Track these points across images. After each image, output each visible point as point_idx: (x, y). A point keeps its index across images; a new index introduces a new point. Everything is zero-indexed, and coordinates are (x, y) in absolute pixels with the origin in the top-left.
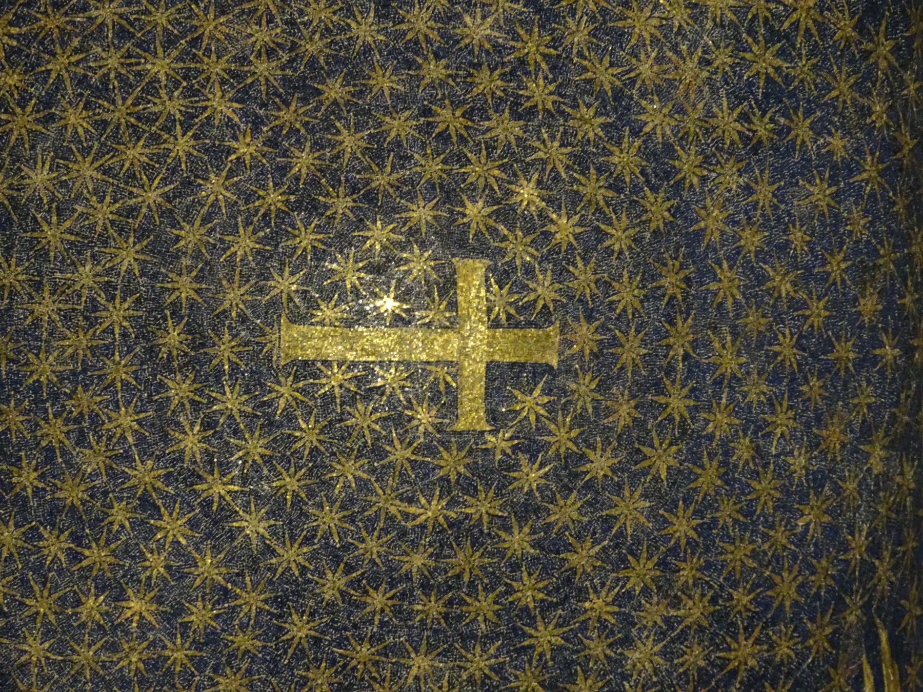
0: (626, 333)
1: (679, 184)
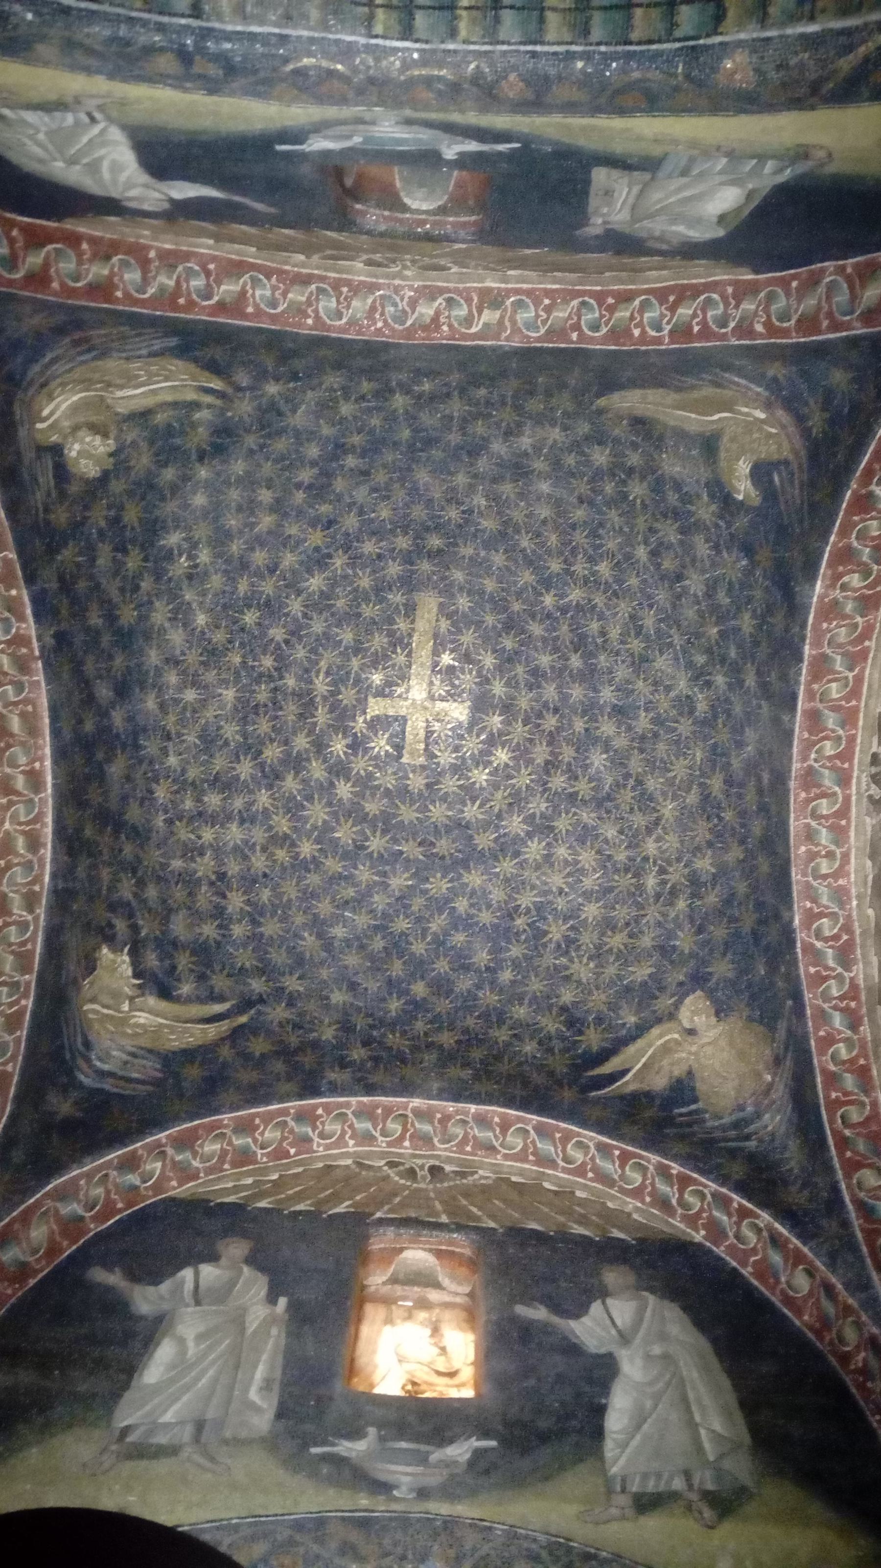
0: (417, 811)
1: (496, 859)
